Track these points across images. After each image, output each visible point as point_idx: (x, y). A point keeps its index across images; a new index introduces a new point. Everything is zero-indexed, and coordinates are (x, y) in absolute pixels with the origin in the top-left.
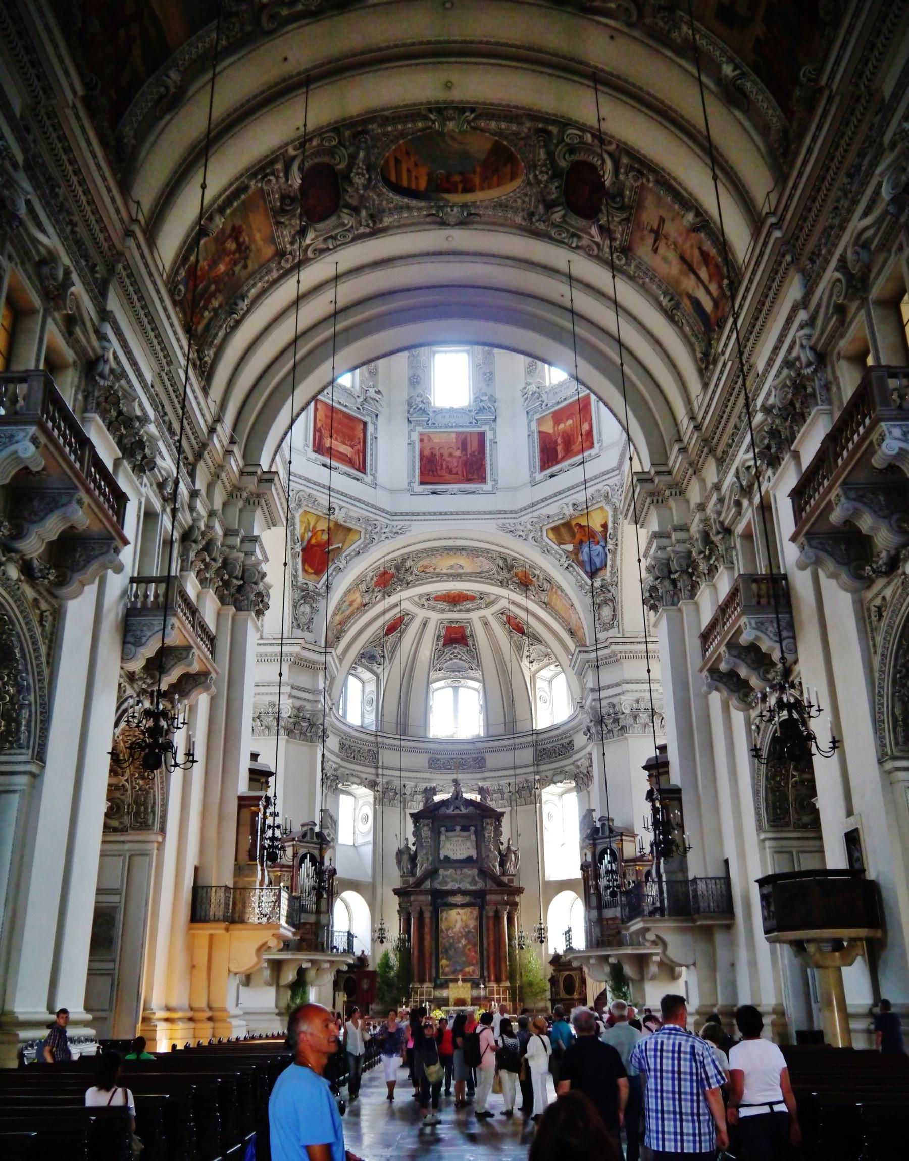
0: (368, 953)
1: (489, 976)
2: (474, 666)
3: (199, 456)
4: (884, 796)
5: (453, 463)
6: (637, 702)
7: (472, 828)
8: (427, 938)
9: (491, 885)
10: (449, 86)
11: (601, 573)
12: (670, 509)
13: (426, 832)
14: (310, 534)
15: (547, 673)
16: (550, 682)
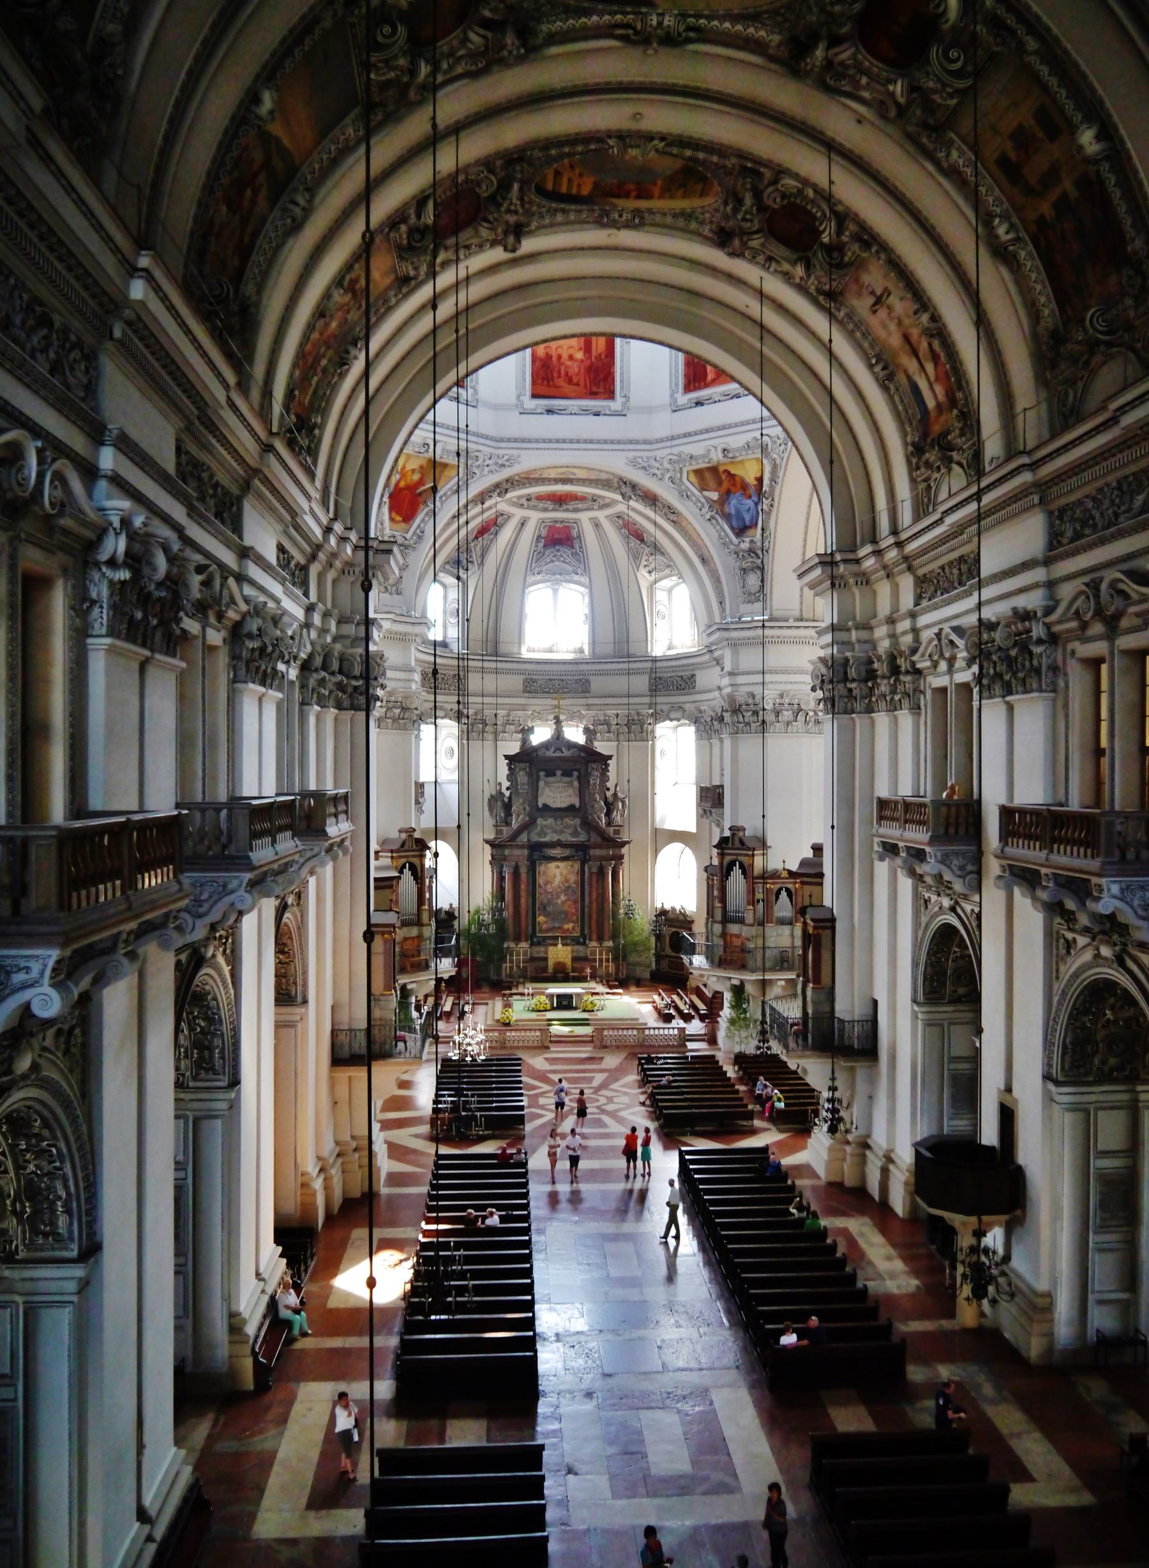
0: (455, 905)
1: (590, 933)
2: (579, 571)
3: (313, 557)
4: (1043, 1111)
5: (574, 368)
6: (782, 696)
7: (576, 773)
8: (523, 894)
9: (595, 838)
10: (637, 116)
11: (750, 532)
12: (854, 595)
13: (522, 778)
14: (398, 476)
15: (666, 583)
16: (670, 591)
